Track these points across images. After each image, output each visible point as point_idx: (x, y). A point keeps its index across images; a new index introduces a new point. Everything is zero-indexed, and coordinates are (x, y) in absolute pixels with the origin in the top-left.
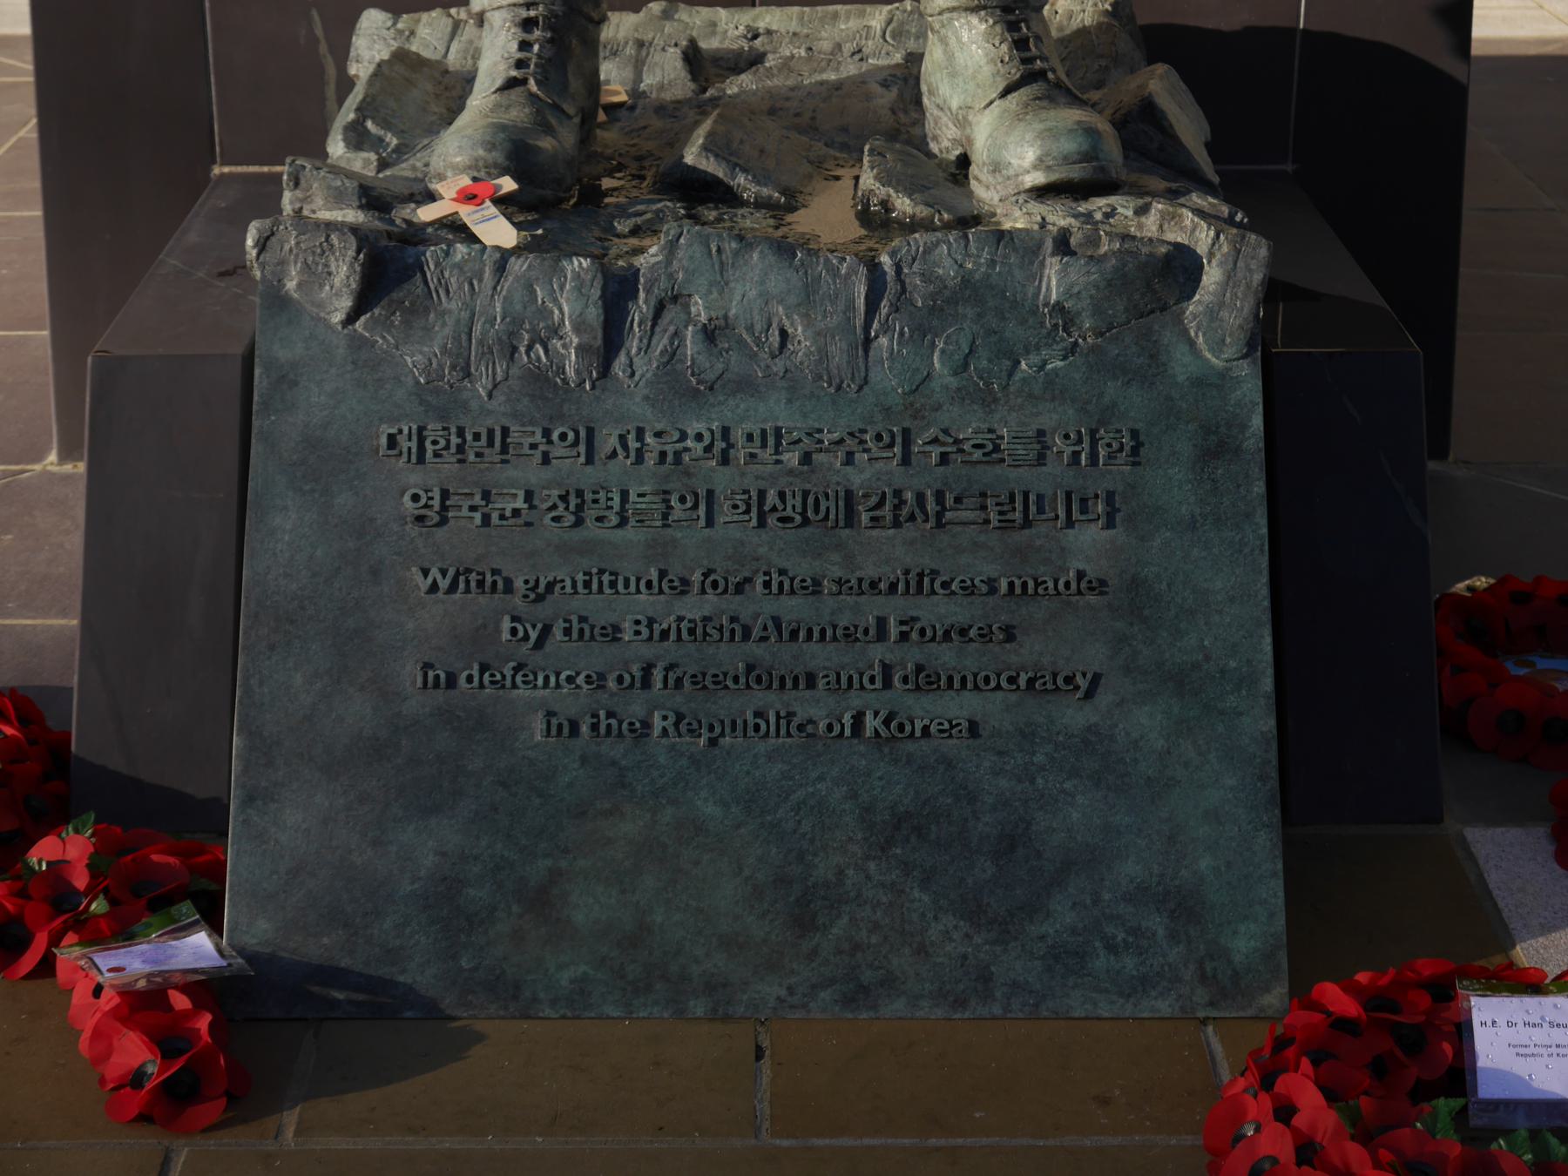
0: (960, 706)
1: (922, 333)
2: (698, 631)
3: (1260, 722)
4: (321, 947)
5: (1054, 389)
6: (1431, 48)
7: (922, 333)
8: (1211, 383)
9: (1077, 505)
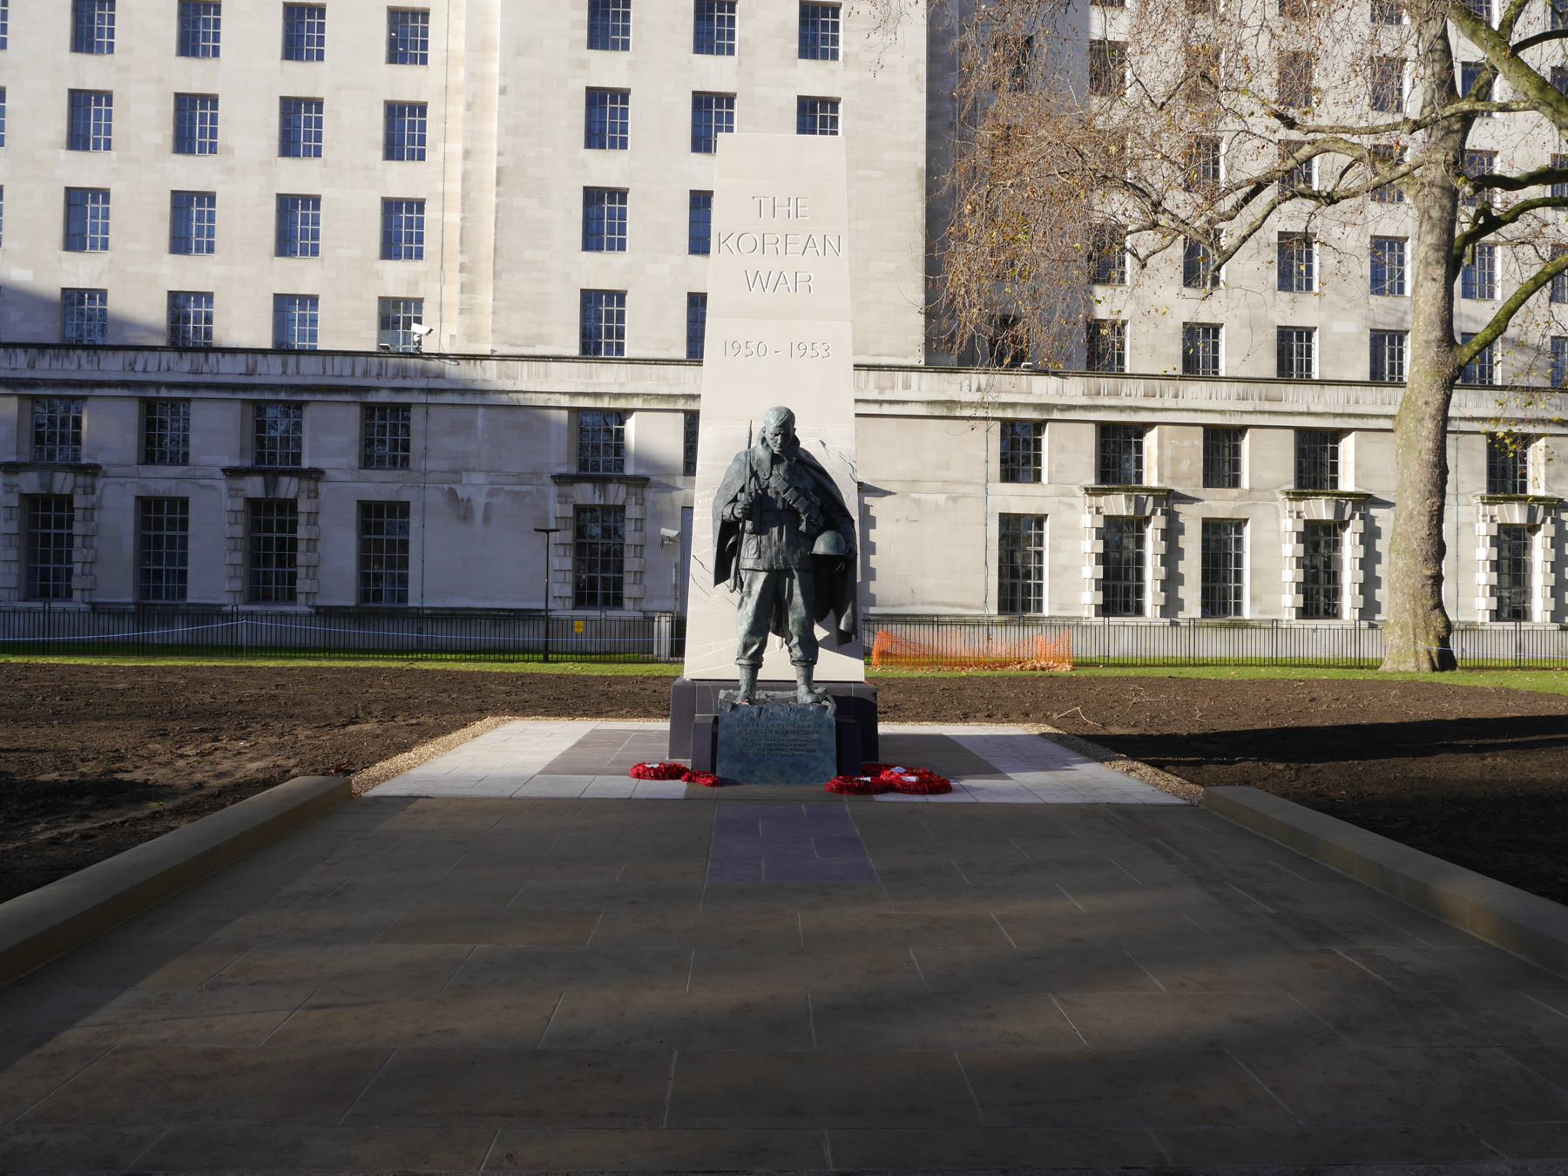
0: (800, 753)
1: (796, 714)
2: (770, 745)
3: (835, 755)
4: (727, 777)
5: (811, 720)
6: (872, 700)
7: (796, 714)
9: (814, 732)
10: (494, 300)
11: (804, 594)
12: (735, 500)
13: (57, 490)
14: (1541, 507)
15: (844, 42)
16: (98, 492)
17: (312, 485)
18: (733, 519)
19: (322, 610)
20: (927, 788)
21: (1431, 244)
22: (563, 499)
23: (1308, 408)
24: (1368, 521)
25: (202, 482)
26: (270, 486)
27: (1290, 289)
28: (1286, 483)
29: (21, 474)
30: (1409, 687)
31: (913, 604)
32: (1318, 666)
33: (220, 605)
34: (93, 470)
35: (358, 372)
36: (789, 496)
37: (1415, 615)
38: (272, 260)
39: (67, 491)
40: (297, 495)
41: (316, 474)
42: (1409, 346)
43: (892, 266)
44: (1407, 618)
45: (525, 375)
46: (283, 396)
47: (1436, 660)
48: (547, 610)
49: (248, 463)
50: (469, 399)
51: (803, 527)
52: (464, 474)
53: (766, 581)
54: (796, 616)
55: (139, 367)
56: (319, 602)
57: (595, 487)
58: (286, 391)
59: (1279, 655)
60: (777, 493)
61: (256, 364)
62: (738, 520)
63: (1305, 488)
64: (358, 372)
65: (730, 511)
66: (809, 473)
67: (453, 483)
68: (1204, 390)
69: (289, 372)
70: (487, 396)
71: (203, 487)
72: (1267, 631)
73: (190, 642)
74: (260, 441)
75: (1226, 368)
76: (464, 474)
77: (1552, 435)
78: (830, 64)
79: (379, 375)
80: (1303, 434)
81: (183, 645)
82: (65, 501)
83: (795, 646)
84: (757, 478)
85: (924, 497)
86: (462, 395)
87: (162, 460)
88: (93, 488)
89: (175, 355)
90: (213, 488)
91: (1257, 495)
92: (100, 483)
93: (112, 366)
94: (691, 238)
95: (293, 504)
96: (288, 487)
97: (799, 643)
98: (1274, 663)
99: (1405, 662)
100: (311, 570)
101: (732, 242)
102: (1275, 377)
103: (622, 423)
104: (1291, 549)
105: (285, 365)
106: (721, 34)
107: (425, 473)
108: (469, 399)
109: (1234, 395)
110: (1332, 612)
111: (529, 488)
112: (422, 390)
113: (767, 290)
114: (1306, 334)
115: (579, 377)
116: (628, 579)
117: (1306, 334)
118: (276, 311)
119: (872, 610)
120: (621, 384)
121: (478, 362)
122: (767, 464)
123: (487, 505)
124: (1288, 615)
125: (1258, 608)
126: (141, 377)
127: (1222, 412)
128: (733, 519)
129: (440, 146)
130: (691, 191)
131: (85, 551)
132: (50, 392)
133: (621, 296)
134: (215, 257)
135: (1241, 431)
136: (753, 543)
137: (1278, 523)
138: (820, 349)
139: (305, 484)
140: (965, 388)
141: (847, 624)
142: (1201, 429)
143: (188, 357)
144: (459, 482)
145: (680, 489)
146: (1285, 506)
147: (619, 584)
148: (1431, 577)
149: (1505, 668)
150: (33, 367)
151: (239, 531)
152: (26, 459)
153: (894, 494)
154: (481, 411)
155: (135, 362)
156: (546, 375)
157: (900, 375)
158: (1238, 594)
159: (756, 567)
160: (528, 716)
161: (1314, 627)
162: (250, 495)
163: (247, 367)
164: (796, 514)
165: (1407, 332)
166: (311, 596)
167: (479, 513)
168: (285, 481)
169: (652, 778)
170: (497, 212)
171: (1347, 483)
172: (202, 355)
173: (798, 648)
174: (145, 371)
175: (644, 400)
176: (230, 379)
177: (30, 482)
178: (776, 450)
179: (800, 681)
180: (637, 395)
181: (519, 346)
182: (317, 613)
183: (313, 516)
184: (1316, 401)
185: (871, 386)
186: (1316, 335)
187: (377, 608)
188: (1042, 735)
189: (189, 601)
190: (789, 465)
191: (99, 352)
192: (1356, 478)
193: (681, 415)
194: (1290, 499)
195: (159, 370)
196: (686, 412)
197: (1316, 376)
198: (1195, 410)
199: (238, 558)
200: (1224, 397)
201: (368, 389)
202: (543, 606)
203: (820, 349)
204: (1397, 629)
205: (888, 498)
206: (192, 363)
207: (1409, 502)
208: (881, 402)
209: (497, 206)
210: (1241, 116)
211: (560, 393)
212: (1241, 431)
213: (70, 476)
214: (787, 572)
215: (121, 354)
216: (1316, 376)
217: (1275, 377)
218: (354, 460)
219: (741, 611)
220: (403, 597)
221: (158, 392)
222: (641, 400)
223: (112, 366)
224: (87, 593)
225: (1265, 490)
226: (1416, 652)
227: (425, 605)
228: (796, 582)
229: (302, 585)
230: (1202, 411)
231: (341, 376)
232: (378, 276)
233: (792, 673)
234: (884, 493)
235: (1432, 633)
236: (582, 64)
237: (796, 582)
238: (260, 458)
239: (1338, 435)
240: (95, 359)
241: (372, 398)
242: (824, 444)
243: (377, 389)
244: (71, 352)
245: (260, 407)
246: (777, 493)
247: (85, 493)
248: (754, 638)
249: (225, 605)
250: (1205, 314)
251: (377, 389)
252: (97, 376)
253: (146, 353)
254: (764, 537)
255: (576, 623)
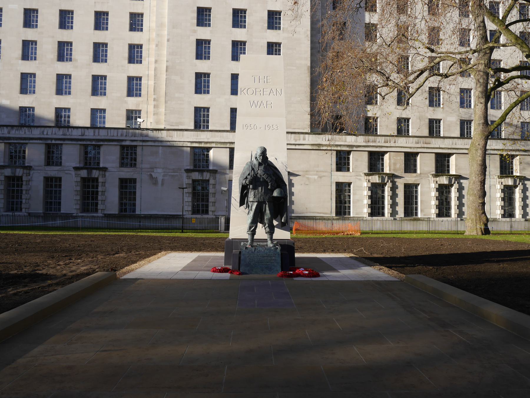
1: (267, 250)
3: (280, 264)
6: (293, 245)
7: (267, 250)
8: (278, 252)
10: (165, 110)
11: (270, 210)
12: (246, 178)
13: (17, 174)
14: (518, 179)
15: (283, 24)
16: (31, 176)
17: (103, 173)
18: (246, 184)
19: (107, 215)
20: (311, 275)
21: (480, 91)
22: (189, 178)
23: (439, 146)
24: (460, 184)
25: (66, 172)
26: (89, 173)
27: (433, 106)
28: (432, 171)
29: (5, 169)
30: (474, 241)
31: (307, 213)
32: (443, 233)
33: (72, 214)
34: (30, 168)
35: (119, 135)
36: (265, 177)
37: (476, 216)
38: (90, 97)
39: (20, 175)
40: (98, 176)
41: (105, 169)
42: (473, 125)
43: (299, 99)
44: (473, 217)
45: (176, 136)
46: (94, 143)
47: (483, 231)
48: (183, 215)
49: (82, 165)
50: (156, 144)
51: (269, 187)
52: (155, 169)
53: (257, 205)
54: (267, 217)
55: (45, 133)
56: (106, 212)
57: (199, 173)
58: (95, 141)
59: (430, 230)
60: (261, 176)
61: (85, 132)
62: (248, 185)
63: (438, 173)
64: (119, 135)
65: (245, 182)
66: (271, 169)
67: (151, 172)
68: (404, 140)
69: (96, 135)
70: (163, 143)
71: (66, 173)
72: (426, 222)
73: (62, 226)
74: (86, 158)
75: (412, 133)
76: (155, 169)
77: (521, 155)
78: (278, 31)
79: (126, 136)
80: (437, 154)
81: (59, 227)
82: (20, 179)
83: (267, 227)
84: (254, 171)
85: (310, 176)
86: (154, 142)
87: (53, 165)
88: (29, 174)
89: (58, 129)
90: (70, 174)
91: (422, 175)
92: (32, 172)
93: (36, 133)
94: (231, 89)
95: (97, 179)
96: (95, 174)
97: (268, 226)
98: (428, 232)
99: (473, 232)
100: (103, 202)
101: (245, 91)
102: (428, 136)
103: (208, 152)
104: (434, 194)
105: (94, 132)
106: (241, 21)
107: (142, 169)
108: (156, 144)
109: (414, 142)
110: (448, 215)
111: (177, 174)
112: (141, 141)
113: (257, 107)
114: (439, 121)
115: (194, 136)
116: (210, 204)
117: (438, 121)
118: (92, 114)
119: (293, 215)
120: (208, 139)
121: (160, 131)
122: (257, 166)
123: (163, 179)
124: (433, 216)
125: (423, 214)
126: (46, 136)
127: (410, 148)
128: (246, 184)
129: (147, 59)
130: (231, 74)
131: (26, 195)
132: (15, 141)
133: (208, 109)
134: (71, 96)
135: (417, 154)
136: (253, 193)
137: (430, 185)
138: (275, 127)
139: (101, 172)
140: (324, 140)
141: (284, 220)
142: (403, 153)
143: (62, 130)
144: (153, 172)
145: (228, 174)
146: (432, 179)
147: (207, 206)
148: (481, 203)
149: (507, 234)
150: (9, 133)
151: (78, 188)
152: (7, 164)
153: (300, 175)
154: (161, 148)
155: (44, 131)
156: (183, 136)
157: (302, 135)
158: (416, 209)
159: (253, 201)
160: (176, 251)
161: (442, 220)
162: (83, 176)
163: (82, 133)
164: (267, 183)
165: (472, 120)
166: (103, 210)
167: (160, 182)
168: (94, 171)
169: (218, 272)
170: (166, 81)
171: (453, 171)
172: (67, 129)
173: (268, 228)
174: (47, 134)
175: (216, 144)
176: (76, 137)
177: (8, 172)
178: (260, 161)
179: (269, 239)
180: (213, 142)
181: (174, 126)
182: (105, 216)
183: (104, 183)
184: (442, 144)
185: (292, 139)
186: (442, 122)
187: (125, 214)
188: (351, 257)
189: (62, 212)
190: (264, 166)
191: (32, 128)
192: (456, 170)
193: (228, 149)
194: (433, 177)
195: (52, 134)
196: (230, 148)
197: (442, 135)
198: (401, 147)
199: (78, 197)
200: (411, 142)
201: (122, 141)
202: (181, 214)
203: (275, 127)
204: (470, 221)
205: (298, 177)
206: (63, 132)
207: (474, 178)
208: (295, 145)
209: (166, 79)
210: (416, 48)
211: (187, 142)
212: (417, 154)
213: (22, 170)
214: (264, 202)
215: (39, 128)
216: (442, 135)
217: (428, 136)
218: (118, 165)
219: (249, 215)
220: (134, 211)
221: (51, 142)
222: (215, 144)
223: (36, 133)
224: (27, 209)
225: (425, 174)
226: (477, 229)
227: (142, 213)
228: (267, 206)
229: (100, 207)
230: (404, 147)
231: (113, 136)
232: (126, 102)
233: (266, 236)
234: (297, 175)
235: (482, 222)
236: (195, 32)
237: (267, 206)
238: (86, 163)
239: (449, 155)
240: (30, 130)
241: (124, 143)
242: (276, 159)
243: (126, 140)
244: (22, 128)
245: (86, 146)
246: (261, 176)
247: (27, 176)
248: (253, 225)
249: (74, 213)
250: (404, 115)
251: (126, 140)
252: (31, 136)
253: (48, 128)
254: (256, 191)
255: (193, 219)
